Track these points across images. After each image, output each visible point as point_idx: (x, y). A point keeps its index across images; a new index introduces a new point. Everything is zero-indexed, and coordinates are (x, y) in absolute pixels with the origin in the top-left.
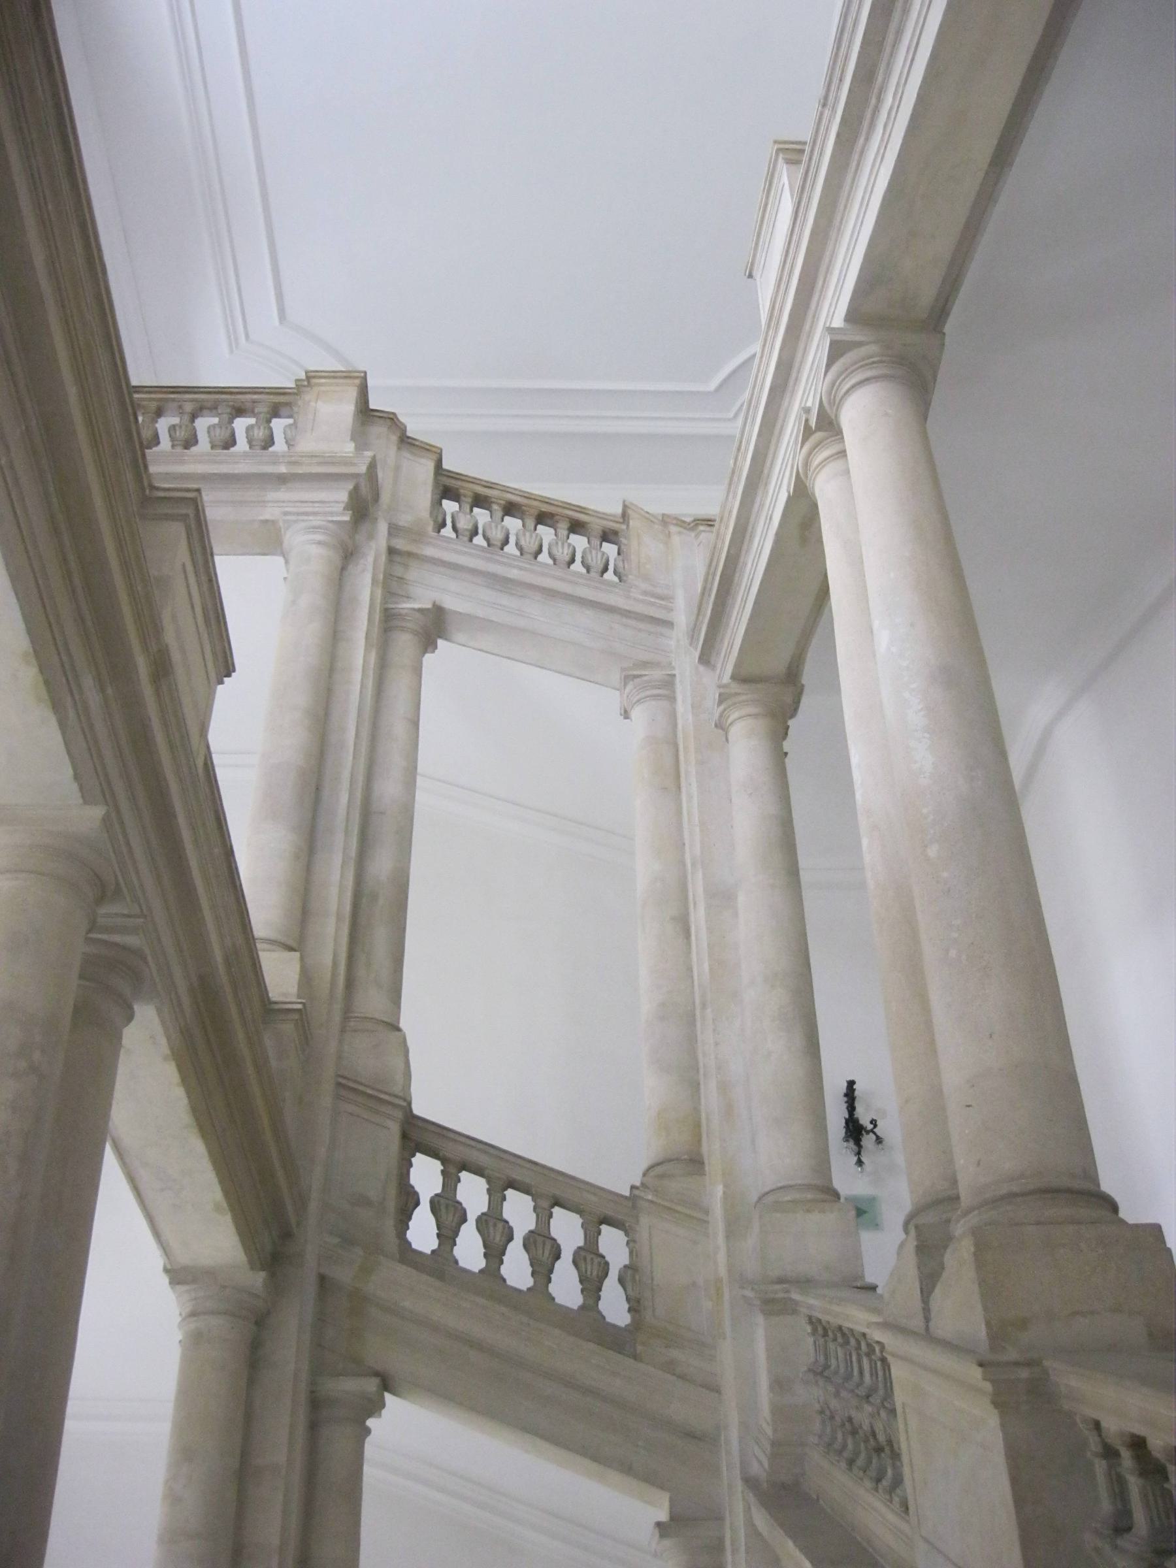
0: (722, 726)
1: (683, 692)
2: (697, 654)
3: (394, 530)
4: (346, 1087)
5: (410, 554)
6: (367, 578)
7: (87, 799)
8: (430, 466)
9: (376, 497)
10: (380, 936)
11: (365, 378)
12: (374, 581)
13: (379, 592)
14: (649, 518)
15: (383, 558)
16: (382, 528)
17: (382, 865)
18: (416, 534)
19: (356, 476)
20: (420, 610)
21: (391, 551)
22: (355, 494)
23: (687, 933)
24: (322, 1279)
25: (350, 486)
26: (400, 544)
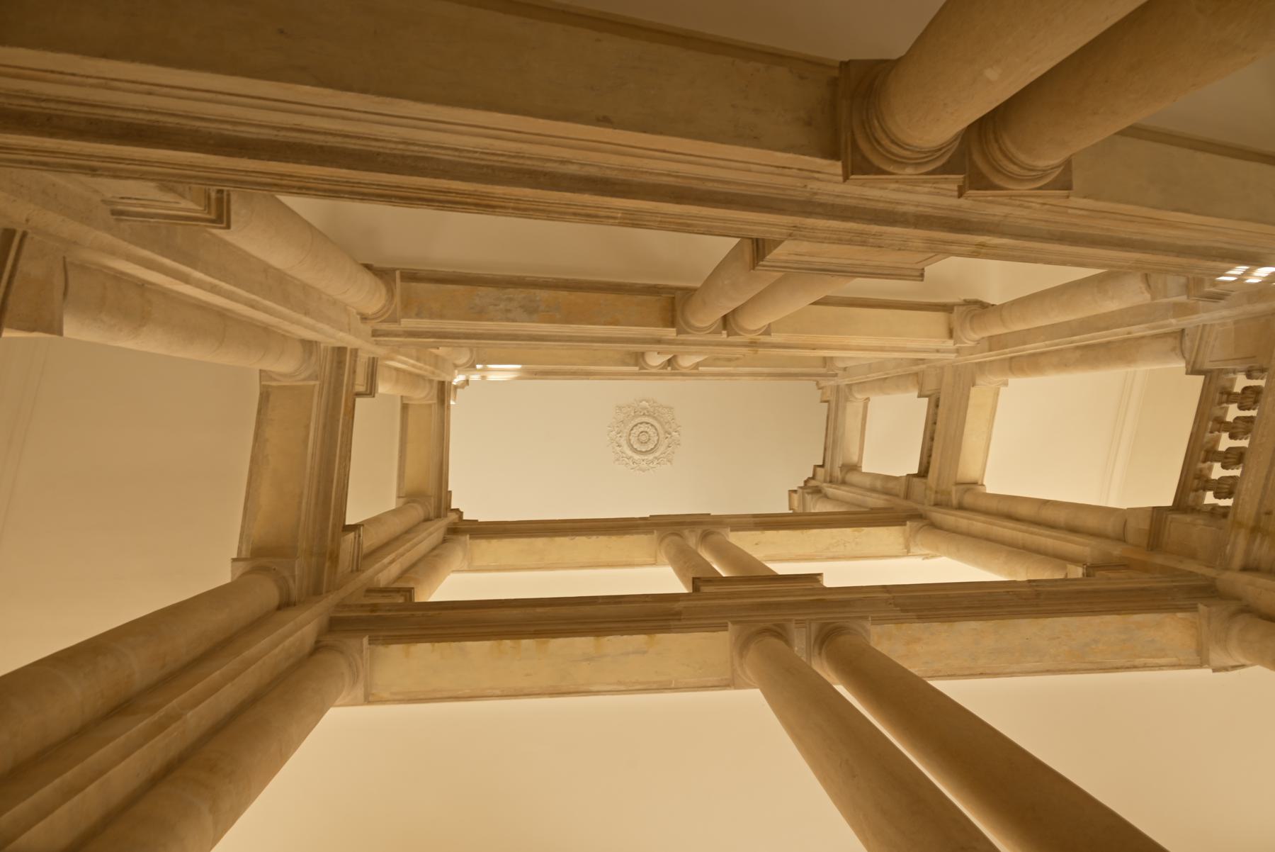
0: (845, 369)
1: (847, 381)
2: (836, 378)
3: (825, 481)
4: (907, 496)
5: (831, 476)
6: (831, 490)
7: (653, 533)
8: (818, 469)
9: (817, 487)
10: (891, 485)
11: (790, 491)
12: (831, 487)
13: (834, 486)
14: (823, 394)
15: (829, 485)
16: (825, 484)
17: (879, 484)
18: (826, 472)
19: (803, 493)
20: (841, 471)
21: (831, 482)
22: (808, 493)
23: (886, 378)
24: (936, 504)
25: (806, 495)
26: (828, 479)
